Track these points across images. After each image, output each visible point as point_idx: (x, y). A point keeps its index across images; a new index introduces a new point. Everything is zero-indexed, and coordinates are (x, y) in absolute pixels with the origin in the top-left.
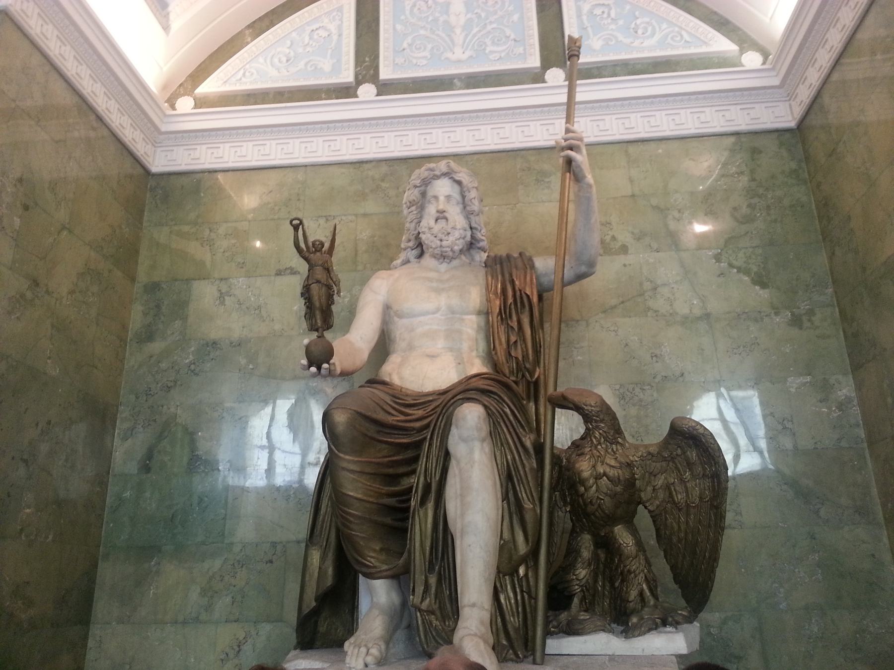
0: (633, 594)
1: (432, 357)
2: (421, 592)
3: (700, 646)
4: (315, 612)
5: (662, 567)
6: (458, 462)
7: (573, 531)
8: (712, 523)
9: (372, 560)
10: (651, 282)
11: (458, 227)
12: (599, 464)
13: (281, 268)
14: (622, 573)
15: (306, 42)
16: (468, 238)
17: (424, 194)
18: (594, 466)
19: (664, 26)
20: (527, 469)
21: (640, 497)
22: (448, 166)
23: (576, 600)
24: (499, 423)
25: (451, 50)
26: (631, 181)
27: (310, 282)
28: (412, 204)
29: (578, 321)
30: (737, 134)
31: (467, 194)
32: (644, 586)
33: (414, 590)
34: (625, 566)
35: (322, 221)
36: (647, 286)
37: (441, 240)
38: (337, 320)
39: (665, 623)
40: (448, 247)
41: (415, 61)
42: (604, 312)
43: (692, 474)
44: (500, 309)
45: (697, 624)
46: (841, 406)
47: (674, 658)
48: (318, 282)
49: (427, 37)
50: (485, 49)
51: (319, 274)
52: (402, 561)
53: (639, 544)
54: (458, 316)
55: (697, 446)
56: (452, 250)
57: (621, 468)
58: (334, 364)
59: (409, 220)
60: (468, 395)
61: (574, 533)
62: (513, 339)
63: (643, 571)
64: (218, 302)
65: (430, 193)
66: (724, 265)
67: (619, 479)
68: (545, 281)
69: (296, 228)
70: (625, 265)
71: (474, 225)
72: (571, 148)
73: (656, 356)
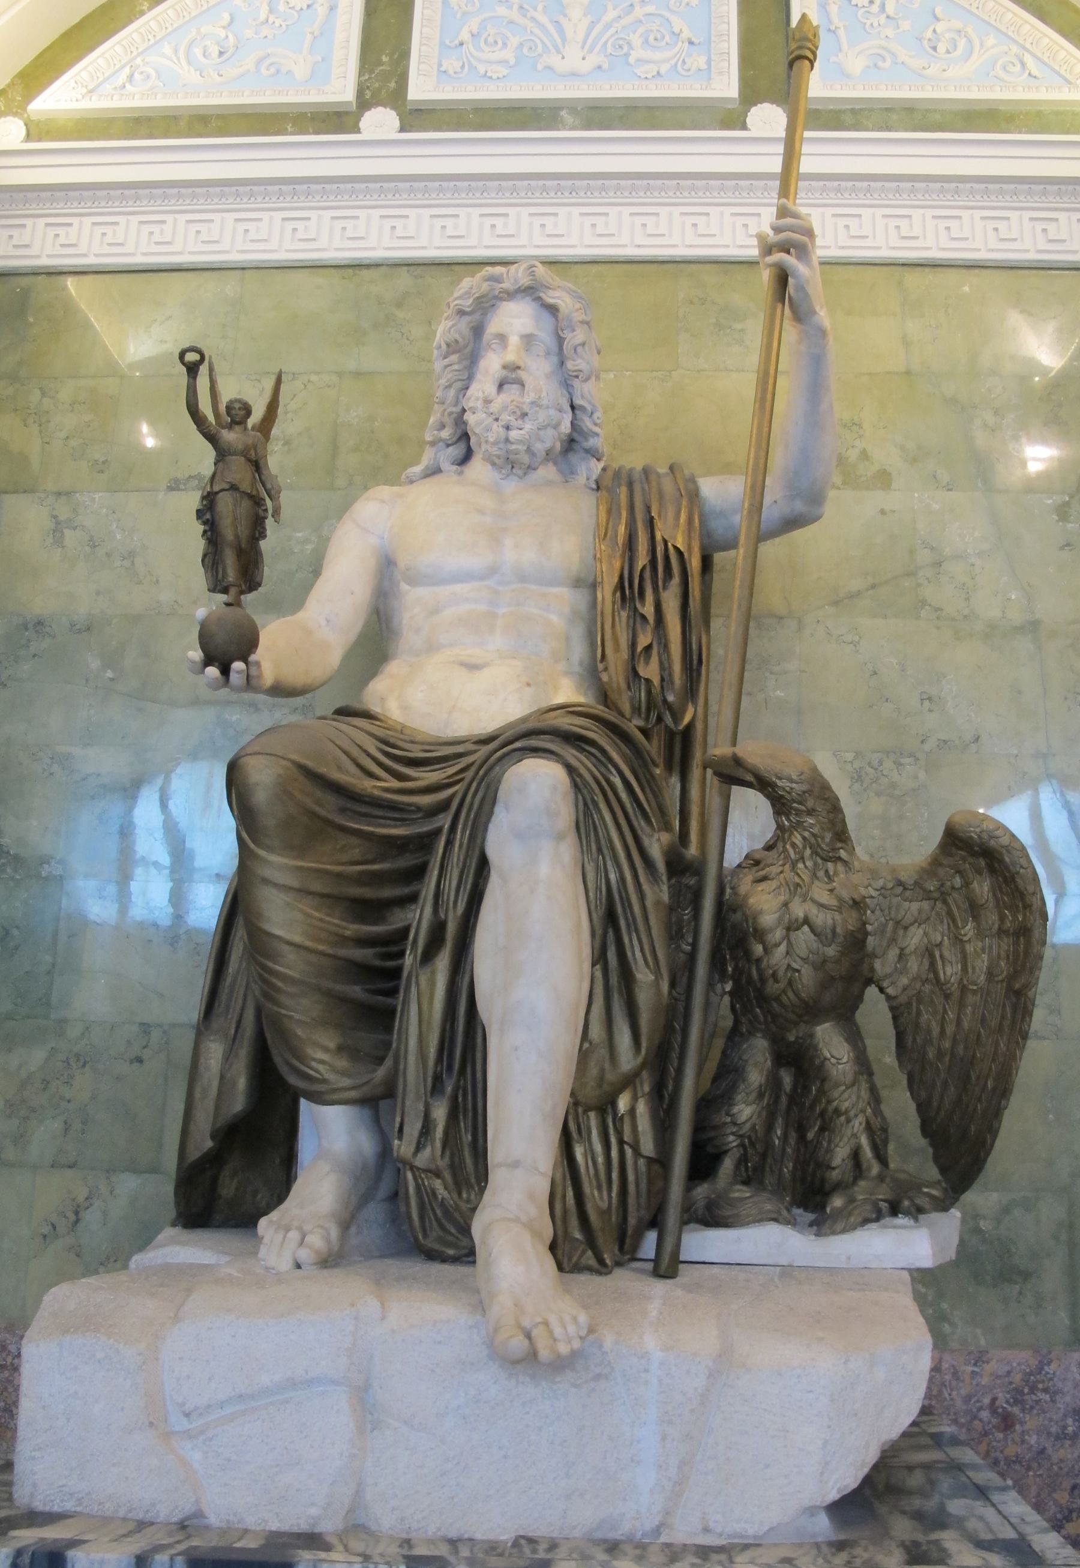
0: (840, 1155)
2: (416, 1133)
3: (958, 1253)
4: (214, 1160)
5: (901, 1107)
7: (735, 1030)
8: (1007, 1023)
9: (321, 1067)
10: (932, 549)
12: (797, 900)
13: (179, 476)
14: (822, 1114)
15: (263, 17)
16: (566, 427)
17: (478, 331)
18: (786, 905)
19: (991, 41)
20: (649, 903)
21: (872, 970)
22: (532, 274)
23: (727, 1165)
24: (596, 804)
25: (558, 52)
26: (906, 342)
27: (216, 488)
29: (781, 618)
31: (567, 335)
32: (864, 1141)
33: (401, 1130)
34: (829, 1102)
36: (924, 556)
37: (508, 428)
38: (270, 571)
39: (895, 1210)
41: (482, 69)
42: (836, 603)
44: (621, 577)
45: (955, 1213)
47: (906, 1275)
48: (233, 488)
49: (511, 22)
50: (627, 55)
51: (239, 472)
52: (381, 1072)
53: (864, 1065)
54: (534, 587)
55: (992, 870)
56: (529, 450)
57: (839, 910)
58: (258, 664)
59: (443, 382)
60: (534, 742)
61: (735, 1036)
62: (644, 640)
63: (863, 1111)
64: (50, 540)
65: (493, 327)
67: (834, 932)
68: (718, 527)
69: (192, 370)
70: (883, 512)
71: (578, 401)
72: (785, 248)
73: (930, 699)
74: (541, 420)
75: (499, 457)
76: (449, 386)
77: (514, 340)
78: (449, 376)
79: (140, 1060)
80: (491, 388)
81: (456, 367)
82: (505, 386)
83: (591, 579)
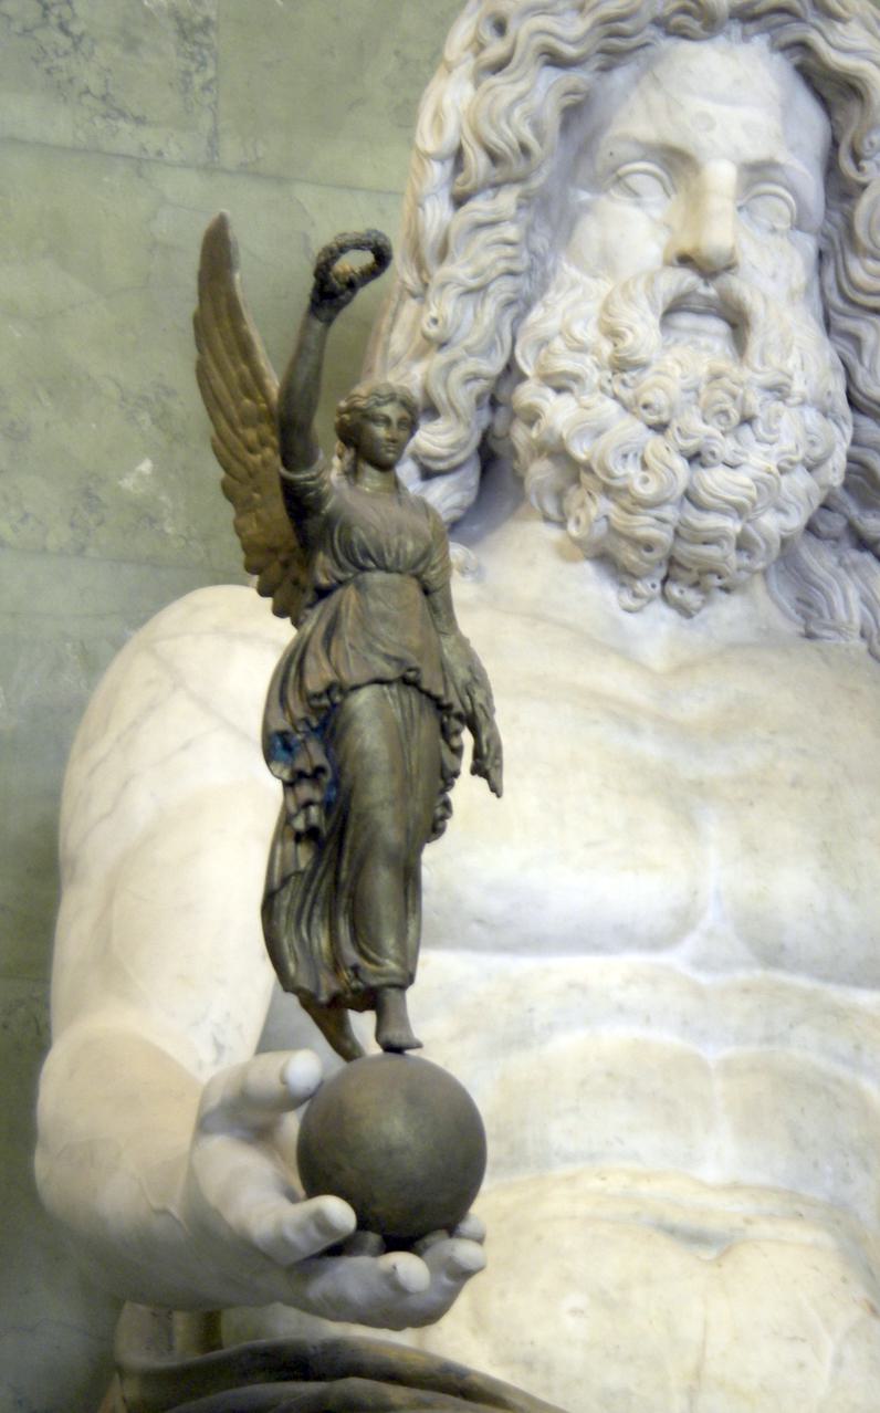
11: (798, 387)
37: (695, 458)
40: (739, 510)
54: (802, 982)
65: (637, 115)
74: (787, 444)
75: (649, 547)
76: (477, 292)
77: (721, 175)
78: (487, 258)
81: (511, 232)
82: (684, 321)
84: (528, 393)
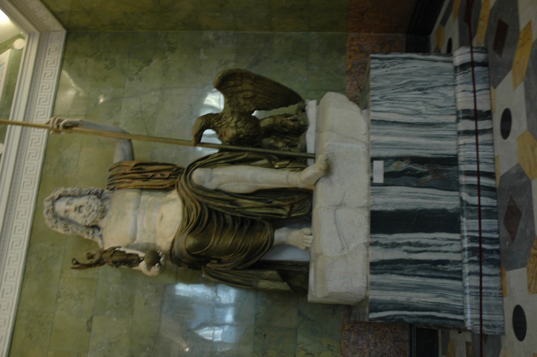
0: (291, 123)
1: (162, 218)
6: (221, 184)
16: (95, 197)
17: (62, 219)
28: (66, 226)
30: (63, 60)
32: (289, 118)
35: (60, 300)
37: (93, 211)
43: (240, 86)
46: (217, 38)
59: (76, 230)
62: (158, 175)
65: (62, 214)
66: (136, 77)
79: (265, 335)
80: (81, 215)
83: (139, 191)
84: (87, 224)
